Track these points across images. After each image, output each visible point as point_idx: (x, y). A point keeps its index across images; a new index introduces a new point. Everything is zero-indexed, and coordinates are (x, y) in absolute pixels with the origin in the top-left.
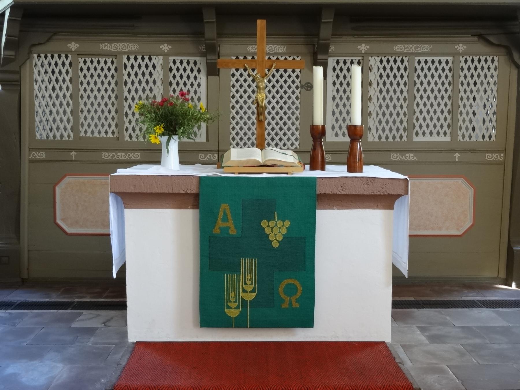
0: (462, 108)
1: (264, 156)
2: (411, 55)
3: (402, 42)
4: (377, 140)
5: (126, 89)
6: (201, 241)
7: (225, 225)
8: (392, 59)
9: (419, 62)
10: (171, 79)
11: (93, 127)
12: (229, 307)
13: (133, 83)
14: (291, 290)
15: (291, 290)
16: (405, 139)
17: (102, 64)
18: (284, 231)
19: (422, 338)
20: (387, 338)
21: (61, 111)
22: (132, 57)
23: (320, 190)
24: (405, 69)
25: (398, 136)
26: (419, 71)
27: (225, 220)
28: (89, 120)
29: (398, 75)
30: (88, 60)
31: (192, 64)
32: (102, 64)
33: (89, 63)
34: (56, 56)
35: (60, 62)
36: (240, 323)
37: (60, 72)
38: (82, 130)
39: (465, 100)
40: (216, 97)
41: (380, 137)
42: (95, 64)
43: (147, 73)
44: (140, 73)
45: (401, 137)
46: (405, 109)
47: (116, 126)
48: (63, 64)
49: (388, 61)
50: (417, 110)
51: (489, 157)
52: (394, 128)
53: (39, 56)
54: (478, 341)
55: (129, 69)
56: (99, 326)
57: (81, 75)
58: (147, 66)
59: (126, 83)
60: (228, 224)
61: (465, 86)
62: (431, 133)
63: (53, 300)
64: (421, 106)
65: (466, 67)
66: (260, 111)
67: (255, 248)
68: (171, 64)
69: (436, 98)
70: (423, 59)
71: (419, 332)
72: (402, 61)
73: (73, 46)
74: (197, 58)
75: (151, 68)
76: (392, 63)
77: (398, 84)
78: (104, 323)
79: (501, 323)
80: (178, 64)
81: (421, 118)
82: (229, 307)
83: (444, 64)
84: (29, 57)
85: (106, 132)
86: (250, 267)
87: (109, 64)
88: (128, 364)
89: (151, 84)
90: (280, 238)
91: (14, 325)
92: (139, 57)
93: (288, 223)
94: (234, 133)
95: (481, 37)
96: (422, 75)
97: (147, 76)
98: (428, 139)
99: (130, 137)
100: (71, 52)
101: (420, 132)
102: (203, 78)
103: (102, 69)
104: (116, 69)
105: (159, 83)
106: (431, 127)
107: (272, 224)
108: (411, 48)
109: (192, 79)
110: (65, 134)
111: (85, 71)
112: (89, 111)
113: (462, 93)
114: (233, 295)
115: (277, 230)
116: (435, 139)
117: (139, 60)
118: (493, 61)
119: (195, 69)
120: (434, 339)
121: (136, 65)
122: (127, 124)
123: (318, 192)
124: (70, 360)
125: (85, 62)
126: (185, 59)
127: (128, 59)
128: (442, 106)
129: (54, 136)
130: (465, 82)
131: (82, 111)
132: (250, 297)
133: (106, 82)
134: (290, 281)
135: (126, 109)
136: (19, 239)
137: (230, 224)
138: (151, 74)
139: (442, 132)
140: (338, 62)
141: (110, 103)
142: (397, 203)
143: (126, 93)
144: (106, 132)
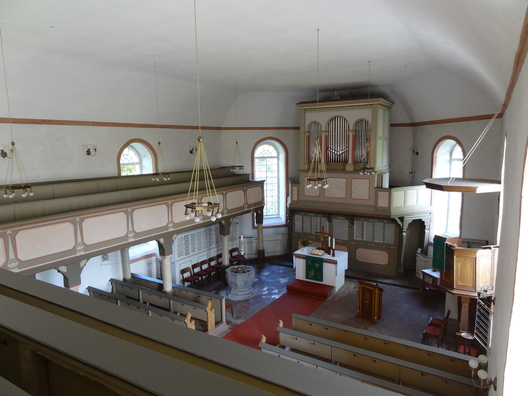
36: (311, 279)
51: (392, 247)
67: (315, 266)
86: (313, 270)
98: (377, 241)
102: (328, 223)
108: (373, 220)
115: (317, 265)
116: (379, 242)
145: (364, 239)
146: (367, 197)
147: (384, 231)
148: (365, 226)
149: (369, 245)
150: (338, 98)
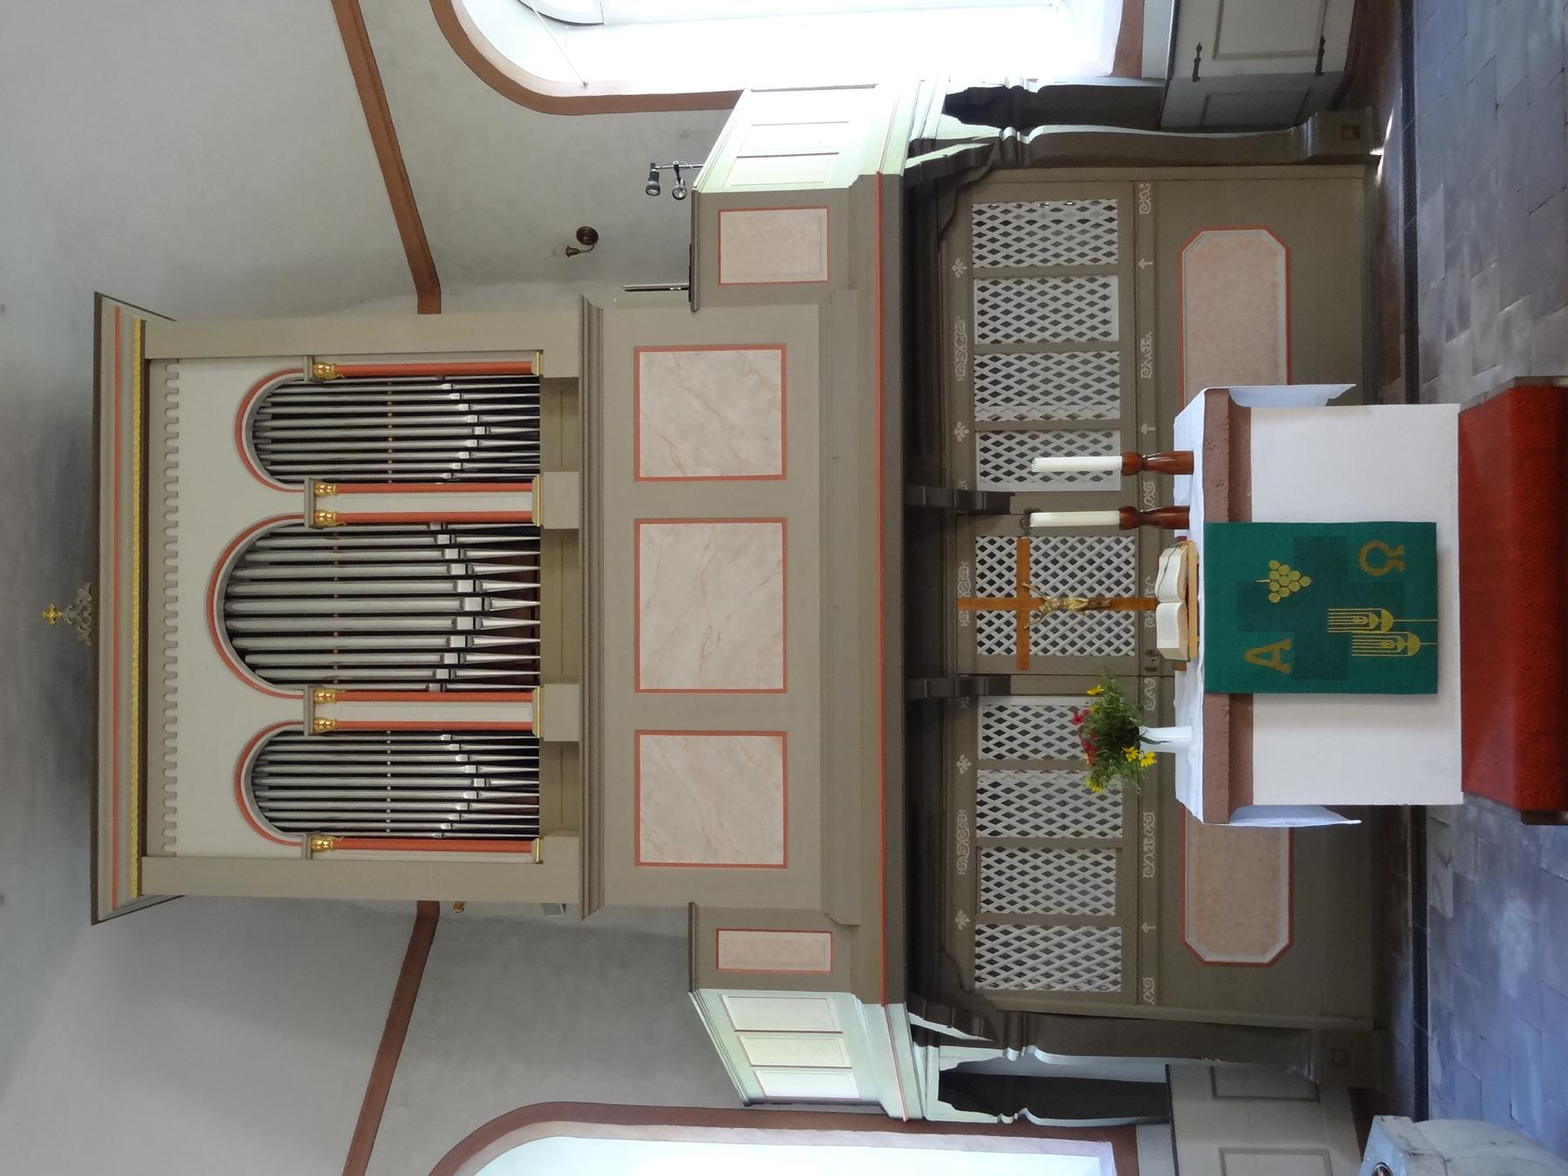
0: (1061, 260)
1: (1170, 599)
2: (972, 350)
3: (952, 366)
4: (1117, 403)
5: (1034, 834)
6: (1302, 691)
7: (1277, 656)
8: (979, 383)
9: (983, 336)
10: (1015, 756)
11: (1099, 893)
12: (1405, 650)
13: (1023, 821)
14: (1376, 558)
15: (1376, 558)
16: (1114, 355)
17: (991, 873)
18: (1285, 568)
19: (1462, 339)
20: (1455, 409)
21: (1071, 946)
22: (980, 821)
23: (1223, 517)
24: (995, 359)
25: (1110, 368)
26: (998, 336)
27: (1268, 656)
28: (1086, 899)
29: (1005, 371)
30: (985, 896)
31: (991, 721)
32: (991, 873)
33: (990, 896)
34: (978, 950)
35: (989, 944)
36: (1431, 633)
37: (1006, 944)
38: (1105, 911)
39: (1047, 255)
40: (1061, 677)
41: (1113, 398)
42: (990, 884)
43: (1005, 797)
44: (1006, 809)
45: (1112, 361)
46: (1063, 357)
47: (1096, 852)
48: (992, 938)
49: (983, 389)
50: (1065, 335)
51: (1145, 209)
52: (1097, 374)
53: (979, 979)
54: (1466, 249)
55: (999, 827)
56: (1450, 871)
57: (1009, 909)
58: (995, 797)
59: (1024, 833)
60: (1276, 652)
61: (1022, 256)
62: (1105, 310)
63: (1411, 964)
64: (1058, 329)
65: (991, 258)
66: (1097, 604)
67: (1313, 612)
68: (990, 755)
69: (1043, 305)
70: (978, 331)
71: (1454, 341)
72: (982, 365)
73: (962, 920)
74: (981, 711)
75: (997, 791)
76: (985, 383)
77: (1021, 370)
78: (1446, 864)
79: (1439, 198)
80: (990, 744)
81: (1078, 329)
82: (1405, 650)
83: (986, 295)
84: (980, 996)
85: (1108, 870)
86: (1341, 619)
87: (990, 861)
88: (1489, 797)
89: (1025, 790)
90: (1296, 575)
91: (1450, 1015)
92: (980, 809)
93: (1274, 564)
94: (1107, 650)
95: (941, 237)
96: (1004, 330)
97: (1011, 797)
98: (1114, 315)
99: (1115, 828)
100: (972, 924)
101: (1103, 328)
102: (1014, 703)
103: (1000, 873)
104: (1000, 850)
105: (1023, 777)
106: (1094, 310)
107: (1274, 587)
108: (960, 351)
109: (1015, 721)
110: (1112, 940)
111: (1003, 902)
112: (1072, 898)
113: (1035, 261)
114: (1385, 644)
115: (1284, 580)
116: (1114, 303)
117: (984, 809)
118: (980, 212)
119: (999, 715)
120: (1464, 321)
121: (992, 815)
122: (1094, 833)
123: (1226, 520)
124: (1499, 903)
125: (988, 902)
126: (982, 733)
127: (982, 828)
128: (1057, 293)
129: (1115, 959)
130: (1017, 257)
131: (1071, 910)
132: (1387, 618)
133: (1021, 867)
134: (1363, 559)
135: (1067, 833)
136: (1300, 1031)
137: (1275, 648)
138: (1008, 791)
139: (1102, 292)
140: (985, 474)
141: (1057, 863)
142: (1241, 403)
143: (1041, 834)
144: (1108, 870)
145: (1113, 411)
146: (769, 362)
147: (1032, 272)
148: (1008, 414)
149: (1147, 371)
150: (83, 593)
